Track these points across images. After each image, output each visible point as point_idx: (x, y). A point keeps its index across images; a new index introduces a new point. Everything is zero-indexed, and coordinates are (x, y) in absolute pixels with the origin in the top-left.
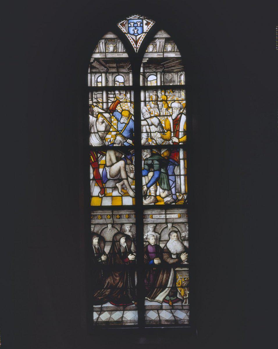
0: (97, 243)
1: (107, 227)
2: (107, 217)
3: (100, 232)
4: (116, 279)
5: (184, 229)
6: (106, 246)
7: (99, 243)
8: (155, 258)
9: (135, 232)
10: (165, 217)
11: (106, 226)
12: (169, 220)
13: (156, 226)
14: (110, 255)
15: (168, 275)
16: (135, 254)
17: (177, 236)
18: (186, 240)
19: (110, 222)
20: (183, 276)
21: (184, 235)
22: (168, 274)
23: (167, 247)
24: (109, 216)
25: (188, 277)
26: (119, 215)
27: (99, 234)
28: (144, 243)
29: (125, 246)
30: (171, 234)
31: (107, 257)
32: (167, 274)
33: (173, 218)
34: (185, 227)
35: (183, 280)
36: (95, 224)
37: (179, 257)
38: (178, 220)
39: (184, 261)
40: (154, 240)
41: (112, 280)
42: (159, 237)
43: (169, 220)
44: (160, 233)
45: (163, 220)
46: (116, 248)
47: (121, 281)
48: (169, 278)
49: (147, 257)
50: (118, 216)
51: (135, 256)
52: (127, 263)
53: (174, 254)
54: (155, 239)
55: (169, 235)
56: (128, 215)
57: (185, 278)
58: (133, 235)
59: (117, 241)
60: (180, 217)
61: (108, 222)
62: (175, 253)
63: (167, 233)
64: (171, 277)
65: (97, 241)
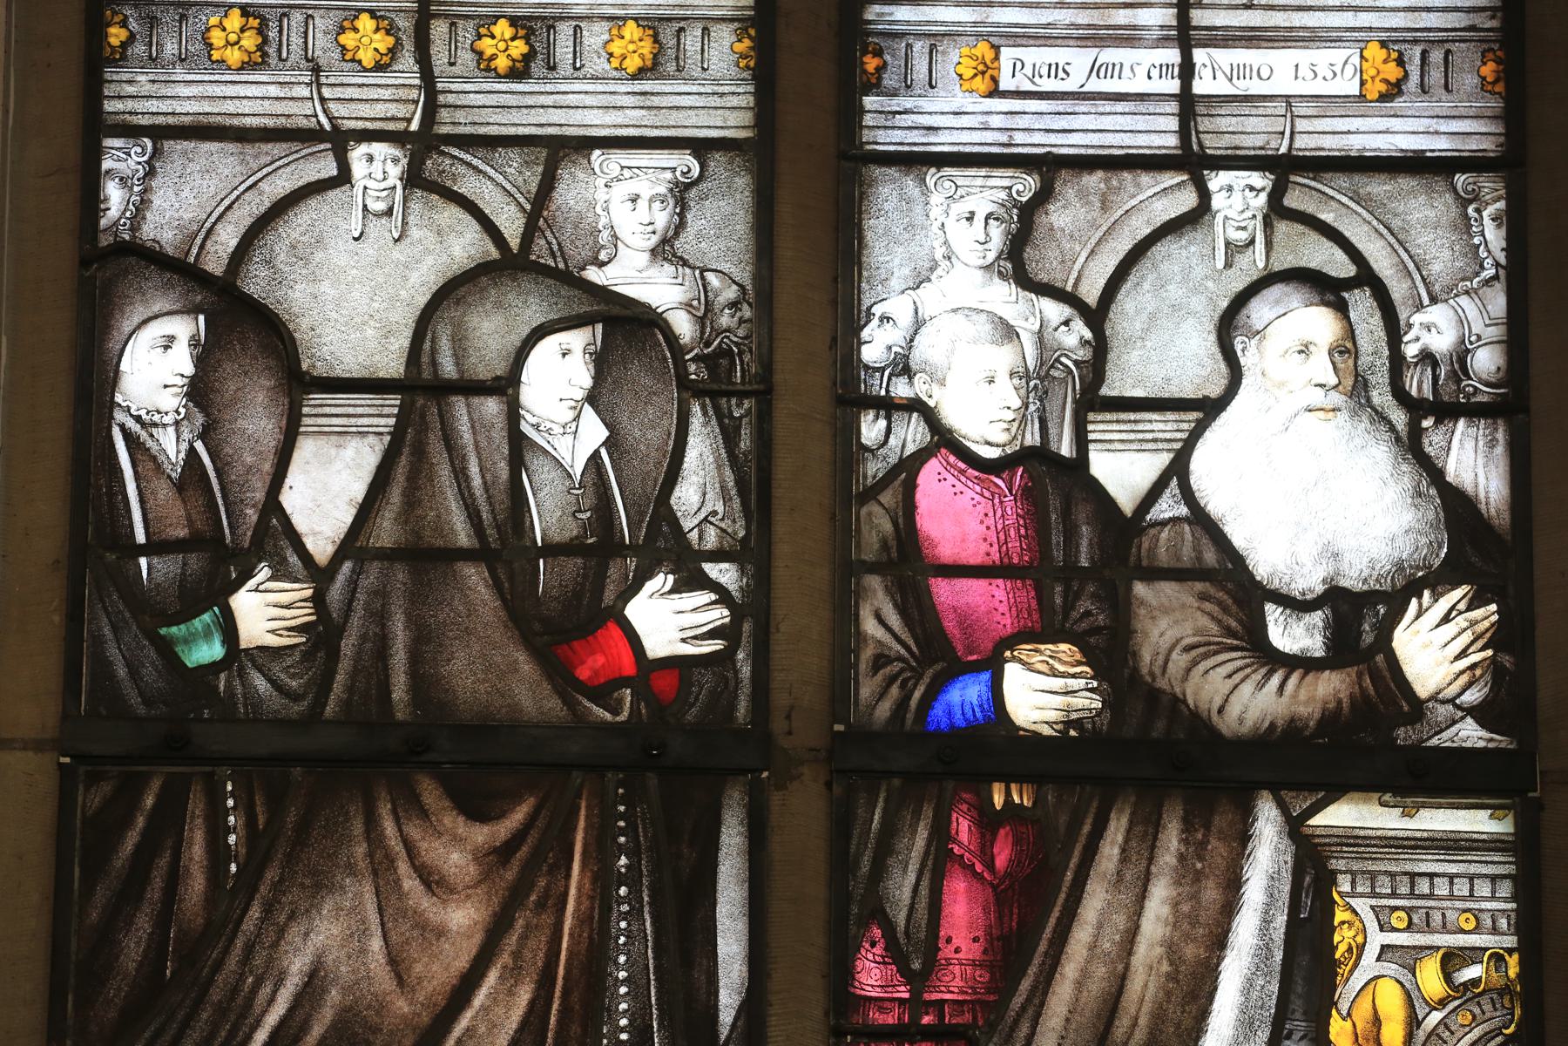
0: (171, 402)
1: (344, 177)
2: (348, 39)
3: (228, 237)
4: (441, 932)
5: (1441, 258)
6: (305, 450)
7: (199, 391)
8: (1011, 641)
9: (744, 275)
10: (1173, 86)
11: (329, 168)
12: (1224, 123)
13: (1044, 196)
14: (370, 580)
15: (1211, 893)
16: (724, 573)
17: (1337, 351)
18: (1474, 412)
19: (380, 110)
20: (1428, 927)
21: (1442, 342)
22: (1198, 877)
23: (1188, 495)
24: (366, 23)
25: (1510, 941)
26: (514, 21)
27: (215, 264)
28: (871, 429)
29: (596, 455)
30: (1260, 311)
31: (318, 600)
32: (1187, 874)
33: (1288, 99)
34: (1464, 226)
35: (1431, 979)
36: (162, 133)
37: (1368, 638)
38: (1355, 123)
39: (1444, 711)
40: (1008, 396)
41: (376, 944)
42: (1084, 354)
43: (1224, 123)
44: (1091, 292)
45: (1140, 123)
46: (460, 474)
47: (505, 958)
48: (1219, 942)
49: (894, 620)
50: (504, 45)
51: (724, 596)
52: (603, 693)
53: (1297, 605)
54: (1022, 375)
55: (1228, 325)
56: (652, 24)
57: (1452, 960)
58: (704, 314)
59: (473, 388)
60: (1394, 90)
61: (352, 115)
62: (1309, 581)
63: (1198, 303)
64: (1246, 930)
65: (182, 362)
